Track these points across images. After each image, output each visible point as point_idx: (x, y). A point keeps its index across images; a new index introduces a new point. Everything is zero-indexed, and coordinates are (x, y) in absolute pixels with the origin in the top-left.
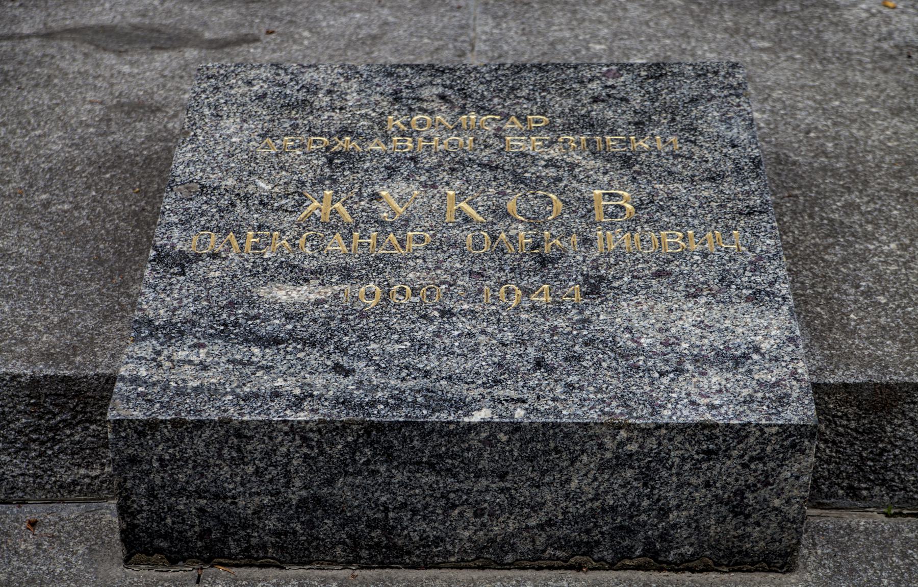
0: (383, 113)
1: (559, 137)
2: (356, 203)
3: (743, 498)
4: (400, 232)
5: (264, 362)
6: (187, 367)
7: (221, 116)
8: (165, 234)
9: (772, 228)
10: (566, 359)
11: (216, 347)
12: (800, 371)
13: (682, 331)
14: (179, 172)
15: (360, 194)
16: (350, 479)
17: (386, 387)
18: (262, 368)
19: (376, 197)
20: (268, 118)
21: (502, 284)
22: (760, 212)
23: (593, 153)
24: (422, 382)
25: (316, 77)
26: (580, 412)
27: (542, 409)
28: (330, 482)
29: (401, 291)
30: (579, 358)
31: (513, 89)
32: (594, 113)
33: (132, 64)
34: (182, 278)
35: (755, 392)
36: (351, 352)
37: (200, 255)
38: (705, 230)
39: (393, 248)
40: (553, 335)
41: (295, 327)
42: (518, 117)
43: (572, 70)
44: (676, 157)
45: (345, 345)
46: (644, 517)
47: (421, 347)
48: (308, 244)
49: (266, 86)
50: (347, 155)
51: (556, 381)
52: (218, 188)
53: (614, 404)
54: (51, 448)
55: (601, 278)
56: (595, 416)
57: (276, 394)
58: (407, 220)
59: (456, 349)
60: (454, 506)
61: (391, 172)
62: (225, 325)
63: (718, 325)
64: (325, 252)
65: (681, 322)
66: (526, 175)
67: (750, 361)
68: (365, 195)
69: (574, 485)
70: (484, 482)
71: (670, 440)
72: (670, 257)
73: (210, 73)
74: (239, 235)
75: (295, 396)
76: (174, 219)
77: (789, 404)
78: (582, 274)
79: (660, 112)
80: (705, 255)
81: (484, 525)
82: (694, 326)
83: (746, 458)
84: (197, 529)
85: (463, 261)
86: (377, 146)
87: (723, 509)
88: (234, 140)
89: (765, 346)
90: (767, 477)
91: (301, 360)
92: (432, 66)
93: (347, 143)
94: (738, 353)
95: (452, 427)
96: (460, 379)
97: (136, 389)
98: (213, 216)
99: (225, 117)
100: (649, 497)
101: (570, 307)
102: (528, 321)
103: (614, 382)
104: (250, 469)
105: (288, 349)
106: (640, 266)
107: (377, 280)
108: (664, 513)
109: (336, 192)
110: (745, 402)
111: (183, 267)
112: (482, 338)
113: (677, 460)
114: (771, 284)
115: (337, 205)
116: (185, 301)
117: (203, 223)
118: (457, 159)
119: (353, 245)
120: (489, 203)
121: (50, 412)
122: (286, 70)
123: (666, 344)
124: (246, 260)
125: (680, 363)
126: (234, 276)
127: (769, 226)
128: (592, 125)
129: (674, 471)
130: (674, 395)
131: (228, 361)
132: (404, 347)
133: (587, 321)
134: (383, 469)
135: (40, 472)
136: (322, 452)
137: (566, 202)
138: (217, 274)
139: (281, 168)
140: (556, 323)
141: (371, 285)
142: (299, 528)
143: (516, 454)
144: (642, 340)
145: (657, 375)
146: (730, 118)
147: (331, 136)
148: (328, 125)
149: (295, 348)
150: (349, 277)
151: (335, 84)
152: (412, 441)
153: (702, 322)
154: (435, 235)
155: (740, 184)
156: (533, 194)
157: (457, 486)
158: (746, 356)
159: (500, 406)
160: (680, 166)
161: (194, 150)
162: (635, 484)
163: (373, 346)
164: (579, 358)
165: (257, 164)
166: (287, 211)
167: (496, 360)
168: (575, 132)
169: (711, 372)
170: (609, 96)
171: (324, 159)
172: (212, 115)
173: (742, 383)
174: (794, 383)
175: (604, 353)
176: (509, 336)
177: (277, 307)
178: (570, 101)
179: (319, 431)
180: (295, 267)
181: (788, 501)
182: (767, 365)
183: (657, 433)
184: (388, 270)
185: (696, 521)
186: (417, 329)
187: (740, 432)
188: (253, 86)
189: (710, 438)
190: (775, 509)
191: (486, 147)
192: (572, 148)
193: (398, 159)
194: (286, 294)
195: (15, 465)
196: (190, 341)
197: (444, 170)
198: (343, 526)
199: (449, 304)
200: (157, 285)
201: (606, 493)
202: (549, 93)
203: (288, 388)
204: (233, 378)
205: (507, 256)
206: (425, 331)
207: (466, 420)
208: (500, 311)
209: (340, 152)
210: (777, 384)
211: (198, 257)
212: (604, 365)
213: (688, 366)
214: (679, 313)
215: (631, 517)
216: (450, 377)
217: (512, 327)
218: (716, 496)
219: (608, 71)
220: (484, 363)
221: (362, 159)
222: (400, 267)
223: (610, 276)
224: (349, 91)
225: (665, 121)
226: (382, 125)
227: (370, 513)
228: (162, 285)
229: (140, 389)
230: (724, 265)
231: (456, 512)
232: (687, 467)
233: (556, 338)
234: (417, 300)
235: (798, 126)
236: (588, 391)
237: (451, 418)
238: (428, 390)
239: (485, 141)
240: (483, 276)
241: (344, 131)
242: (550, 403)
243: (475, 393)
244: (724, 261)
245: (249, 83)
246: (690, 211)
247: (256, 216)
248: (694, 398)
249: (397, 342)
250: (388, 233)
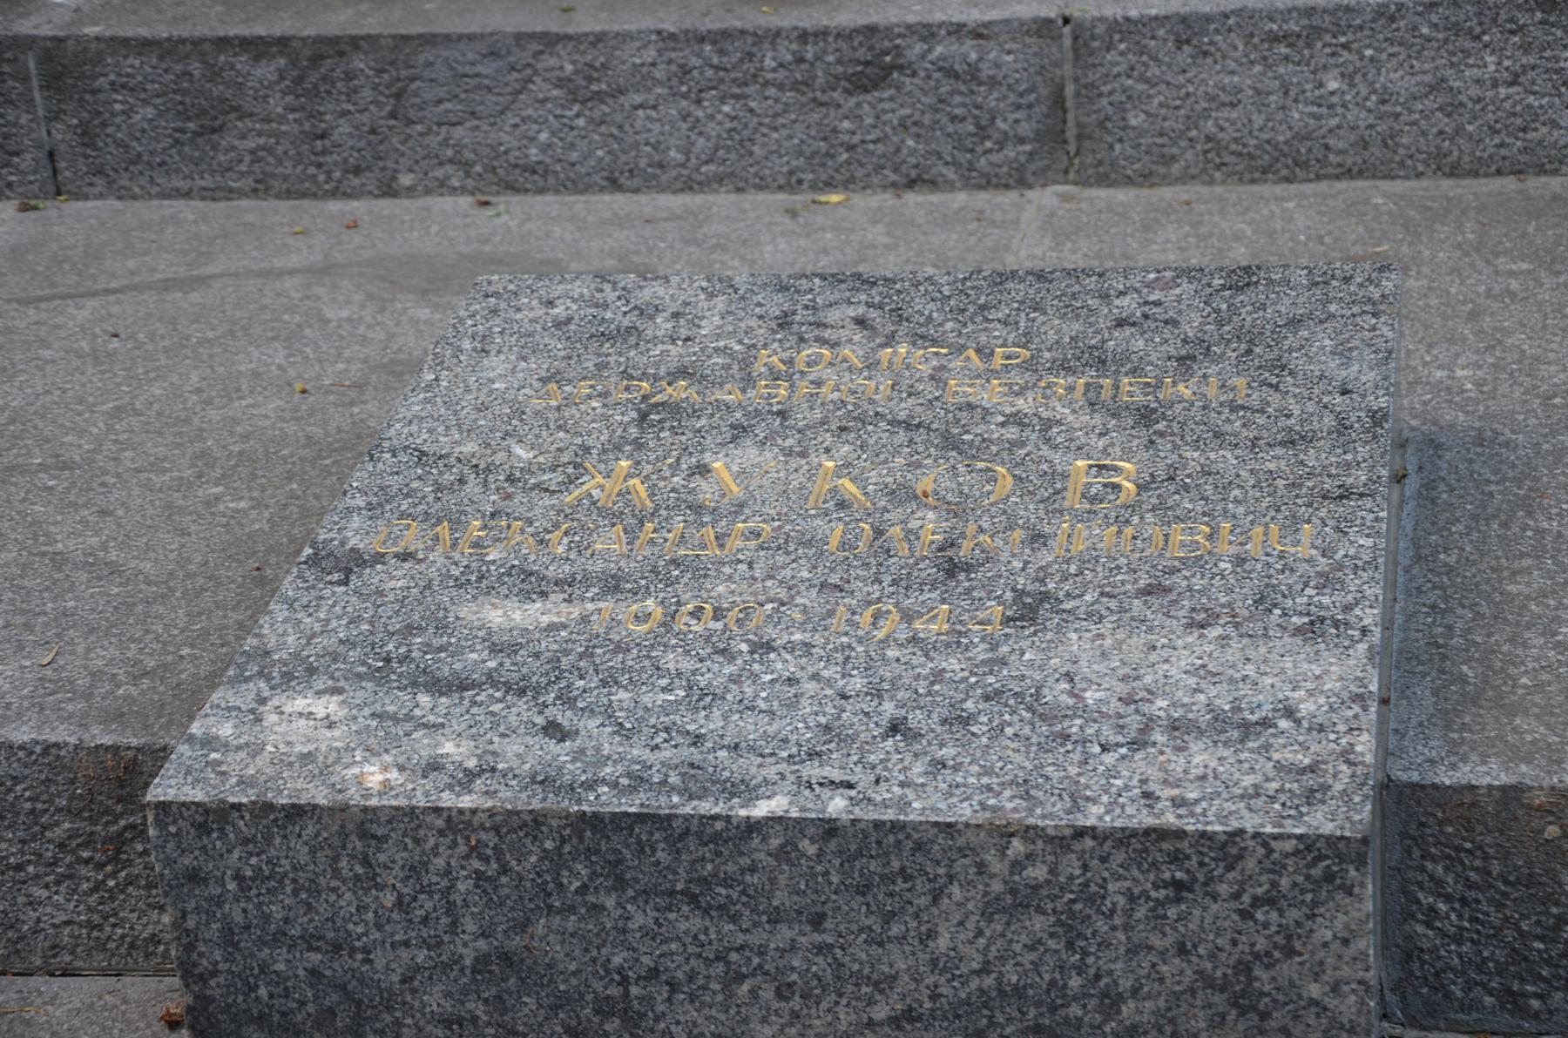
0: (754, 346)
2: (665, 479)
3: (1251, 979)
6: (303, 722)
7: (487, 352)
9: (1377, 519)
10: (944, 722)
11: (361, 693)
12: (1359, 748)
13: (1163, 681)
16: (557, 920)
17: (622, 759)
18: (425, 726)
19: (703, 470)
20: (563, 353)
21: (870, 603)
22: (1361, 495)
23: (1092, 404)
24: (689, 753)
26: (942, 806)
27: (879, 799)
28: (523, 926)
29: (697, 613)
30: (966, 721)
31: (983, 308)
33: (435, 307)
34: (343, 589)
35: (1267, 780)
36: (580, 705)
37: (383, 555)
38: (1252, 523)
39: (705, 547)
40: (933, 683)
41: (501, 664)
42: (978, 351)
43: (1094, 278)
44: (1234, 408)
45: (575, 693)
46: (1075, 1010)
48: (565, 541)
49: (575, 307)
50: (673, 408)
51: (916, 755)
53: (1007, 793)
54: (114, 875)
55: (1045, 596)
56: (968, 812)
58: (741, 506)
60: (740, 978)
61: (739, 432)
62: (388, 660)
63: (1231, 672)
65: (1166, 667)
66: (965, 437)
67: (1272, 731)
69: (943, 942)
70: (786, 933)
71: (1104, 860)
72: (1177, 563)
73: (491, 289)
74: (457, 524)
76: (360, 502)
77: (1323, 802)
78: (1014, 590)
79: (1229, 341)
80: (1240, 561)
81: (796, 1015)
83: (1246, 898)
84: (311, 1008)
86: (728, 395)
87: (1218, 998)
88: (497, 386)
89: (1306, 708)
90: (1289, 937)
91: (493, 714)
92: (858, 276)
93: (680, 391)
94: (1254, 718)
95: (719, 826)
96: (752, 749)
97: (206, 756)
98: (424, 497)
99: (493, 353)
100: (1080, 969)
101: (976, 640)
102: (898, 660)
103: (1018, 758)
104: (389, 899)
107: (661, 595)
108: (1111, 1002)
110: (1242, 797)
112: (810, 687)
113: (1121, 901)
114: (1347, 608)
116: (334, 624)
117: (403, 508)
118: (855, 414)
119: (638, 543)
121: (107, 812)
122: (615, 284)
123: (1127, 700)
124: (456, 564)
125: (1146, 729)
126: (428, 586)
127: (1371, 516)
128: (1104, 362)
129: (1117, 921)
130: (1118, 782)
134: (610, 902)
135: (96, 919)
136: (505, 869)
137: (1021, 479)
138: (400, 584)
139: (560, 427)
140: (944, 664)
141: (650, 602)
142: (481, 1012)
143: (835, 879)
144: (1088, 694)
145: (1097, 749)
148: (657, 365)
150: (617, 589)
151: (687, 304)
152: (654, 850)
153: (1203, 666)
154: (780, 528)
155: (1339, 451)
157: (740, 939)
158: (1266, 723)
159: (807, 792)
160: (1238, 423)
162: (1051, 943)
163: (622, 695)
164: (966, 721)
165: (522, 420)
166: (547, 490)
168: (1070, 370)
170: (1146, 317)
171: (634, 414)
172: (475, 349)
173: (1247, 765)
174: (1344, 767)
177: (480, 634)
178: (1077, 326)
179: (496, 829)
180: (531, 574)
181: (1335, 988)
182: (1301, 738)
183: (1077, 846)
184: (685, 580)
185: (1172, 1021)
187: (1227, 848)
189: (1176, 858)
190: (1313, 1002)
191: (910, 395)
192: (1061, 400)
194: (503, 615)
195: (57, 906)
196: (321, 683)
198: (555, 1009)
199: (770, 632)
200: (297, 600)
201: (1002, 959)
202: (1045, 313)
205: (893, 560)
206: (715, 674)
207: (743, 813)
209: (663, 404)
210: (1312, 769)
211: (379, 558)
212: (1009, 731)
213: (1158, 737)
214: (1165, 653)
215: (1054, 1008)
216: (736, 746)
218: (1200, 973)
219: (1157, 279)
220: (801, 725)
221: (696, 413)
222: (705, 576)
225: (1234, 355)
226: (746, 363)
227: (598, 986)
229: (214, 755)
230: (1270, 577)
231: (745, 987)
232: (1140, 913)
233: (937, 687)
234: (719, 625)
235: (1535, 387)
237: (716, 810)
238: (692, 765)
241: (683, 372)
242: (895, 789)
243: (771, 772)
244: (1272, 571)
245: (550, 303)
246: (1236, 492)
249: (664, 690)
250: (703, 525)
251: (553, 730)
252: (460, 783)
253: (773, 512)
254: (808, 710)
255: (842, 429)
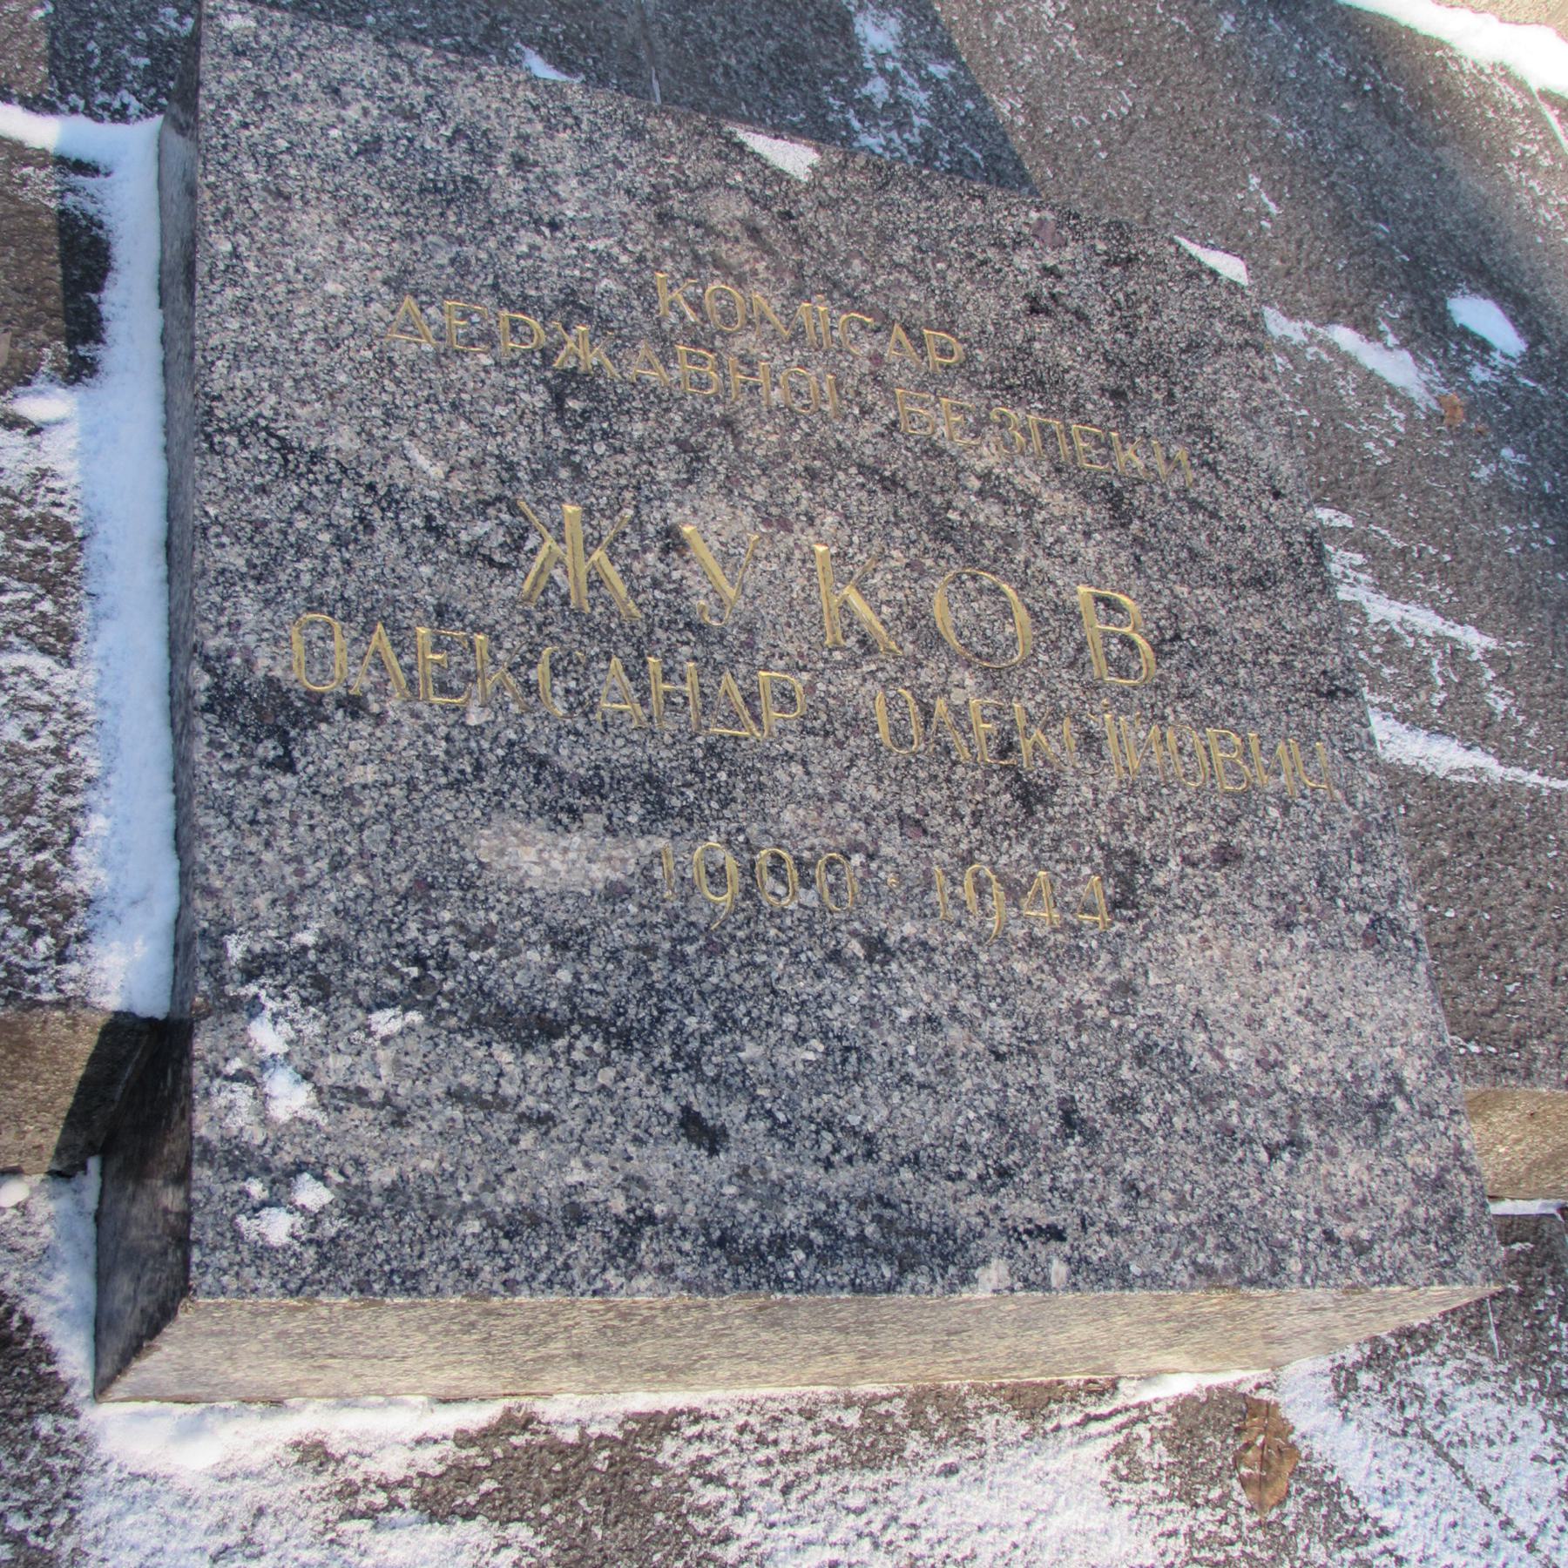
0: (640, 260)
1: (989, 407)
2: (634, 554)
4: (742, 669)
5: (529, 1101)
6: (357, 1112)
7: (288, 198)
8: (221, 611)
14: (218, 386)
15: (638, 524)
19: (672, 542)
22: (1345, 691)
23: (1059, 470)
25: (481, 104)
27: (1095, 1258)
29: (777, 867)
32: (1037, 345)
34: (288, 780)
35: (1415, 1203)
36: (710, 1071)
37: (319, 699)
40: (1079, 1029)
41: (577, 976)
42: (907, 330)
44: (1195, 506)
45: (694, 1044)
47: (847, 1056)
51: (1106, 1173)
52: (316, 457)
53: (1211, 1241)
57: (577, 1216)
59: (912, 1067)
64: (598, 716)
67: (1394, 1117)
68: (651, 529)
75: (618, 1220)
76: (235, 558)
78: (1102, 847)
82: (1299, 1012)
85: (880, 779)
86: (643, 366)
88: (331, 287)
89: (1409, 1074)
93: (581, 349)
96: (936, 1163)
98: (326, 559)
105: (577, 1056)
106: (1190, 828)
107: (723, 824)
109: (588, 511)
111: (285, 740)
112: (955, 1033)
115: (599, 555)
116: (312, 873)
119: (653, 700)
120: (900, 596)
122: (411, 65)
124: (429, 729)
126: (411, 785)
128: (1041, 383)
130: (1298, 1214)
131: (449, 1093)
132: (811, 1056)
133: (1125, 988)
138: (369, 774)
141: (713, 840)
145: (1263, 1156)
146: (1256, 411)
147: (547, 316)
148: (534, 275)
149: (589, 1051)
153: (1310, 1001)
156: (974, 578)
158: (1385, 1104)
159: (1019, 1249)
161: (242, 308)
163: (751, 1051)
165: (398, 382)
166: (491, 562)
167: (991, 1102)
169: (1344, 1147)
170: (1053, 296)
174: (1462, 1178)
175: (1172, 1089)
176: (1001, 1029)
180: (542, 763)
186: (827, 997)
188: (345, 105)
193: (695, 419)
197: (794, 473)
199: (878, 918)
203: (598, 1194)
204: (470, 1157)
205: (960, 770)
208: (975, 948)
210: (1439, 1184)
211: (315, 700)
216: (916, 1154)
217: (1005, 999)
219: (1041, 222)
220: (972, 1115)
222: (760, 787)
223: (1146, 855)
224: (559, 168)
228: (246, 803)
233: (1084, 1038)
234: (809, 898)
236: (1162, 1202)
238: (880, 1198)
239: (858, 394)
240: (925, 832)
241: (573, 305)
242: (1106, 1239)
246: (1242, 672)
247: (426, 570)
248: (1331, 1221)
250: (718, 668)
251: (700, 1131)
252: (624, 1252)
253: (790, 648)
254: (968, 1084)
255: (812, 474)
